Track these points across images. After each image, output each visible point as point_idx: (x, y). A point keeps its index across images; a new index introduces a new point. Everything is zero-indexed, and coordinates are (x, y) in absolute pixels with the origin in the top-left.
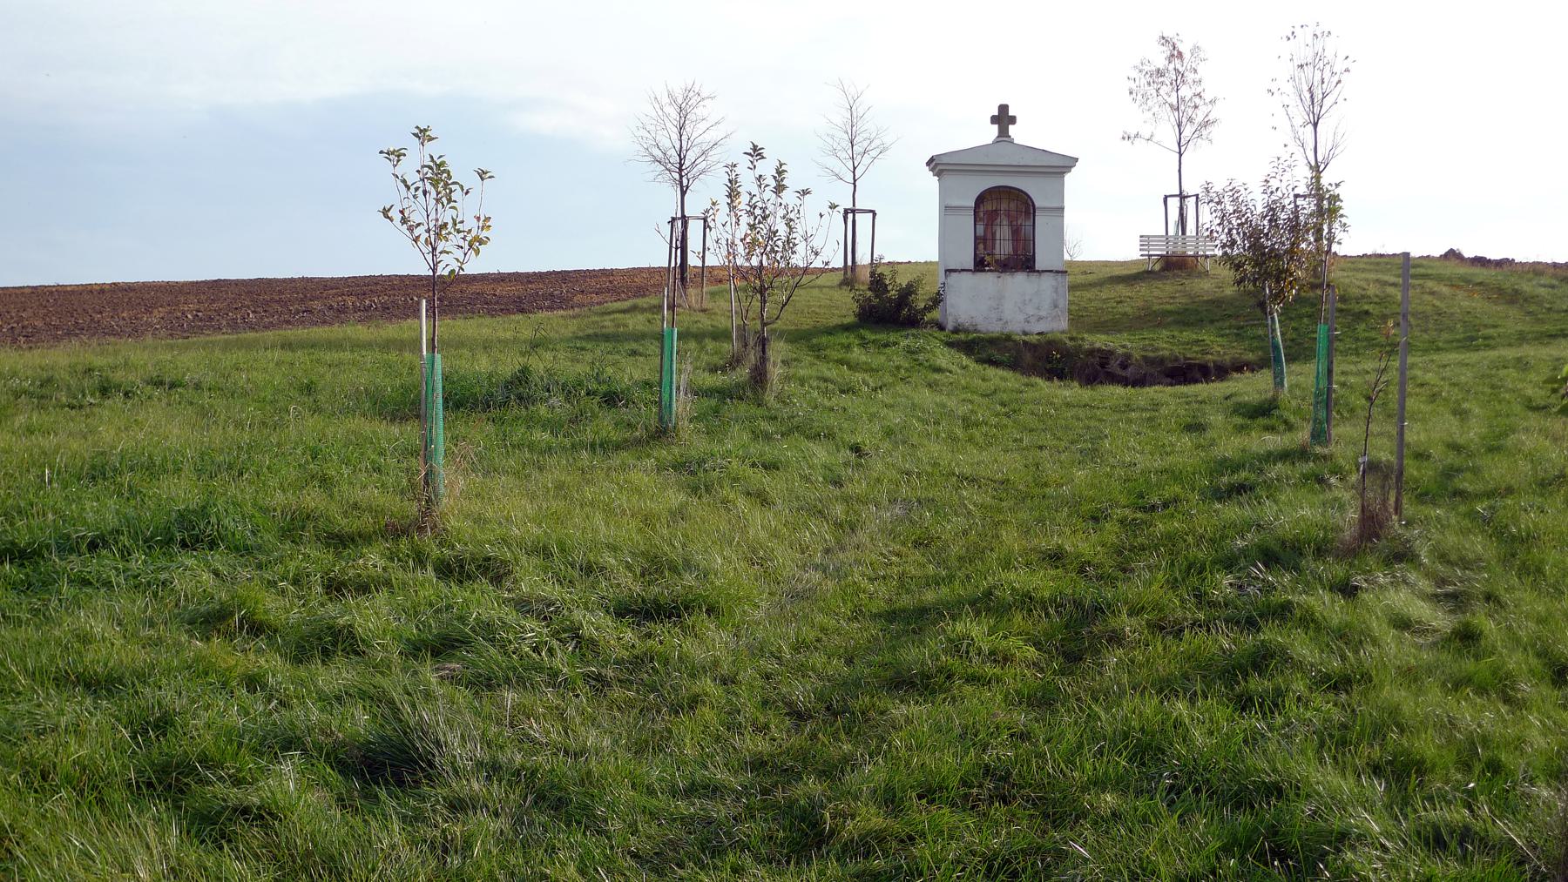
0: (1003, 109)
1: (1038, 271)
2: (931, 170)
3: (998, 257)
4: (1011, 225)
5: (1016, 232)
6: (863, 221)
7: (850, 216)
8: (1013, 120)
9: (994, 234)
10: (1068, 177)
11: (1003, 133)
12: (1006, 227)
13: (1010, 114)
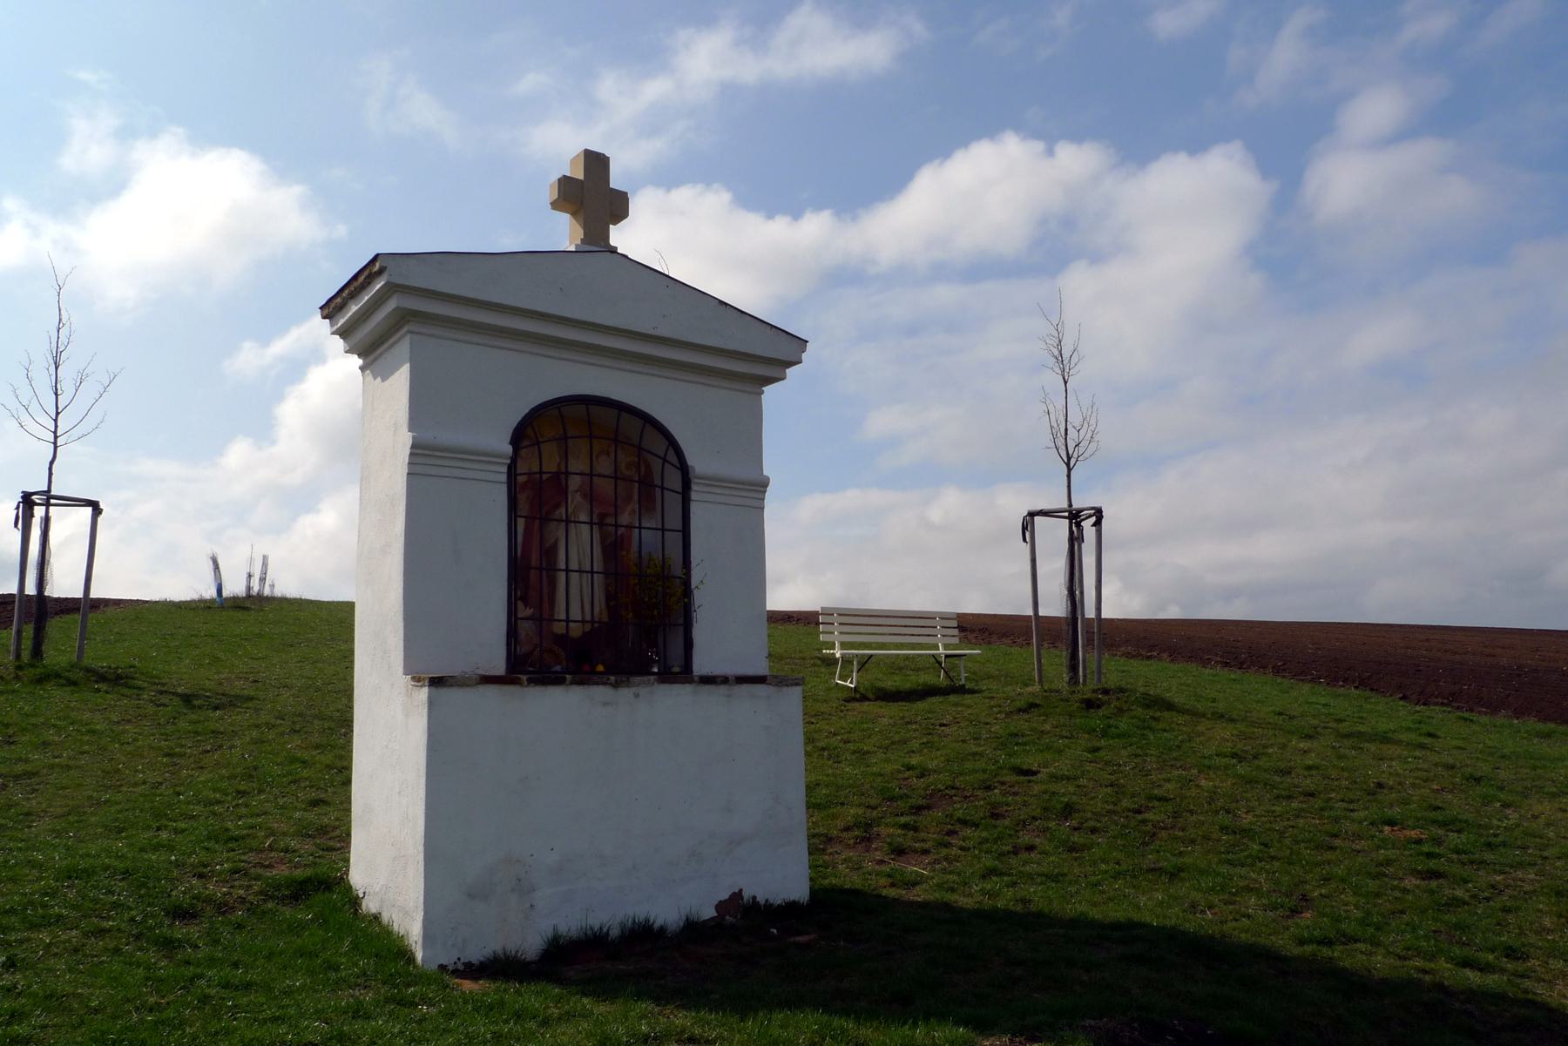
0: (596, 163)
1: (708, 680)
2: (344, 333)
3: (559, 628)
4: (598, 522)
5: (613, 548)
6: (68, 525)
7: (39, 512)
8: (617, 207)
9: (550, 553)
10: (770, 393)
11: (596, 239)
12: (585, 529)
13: (615, 183)
